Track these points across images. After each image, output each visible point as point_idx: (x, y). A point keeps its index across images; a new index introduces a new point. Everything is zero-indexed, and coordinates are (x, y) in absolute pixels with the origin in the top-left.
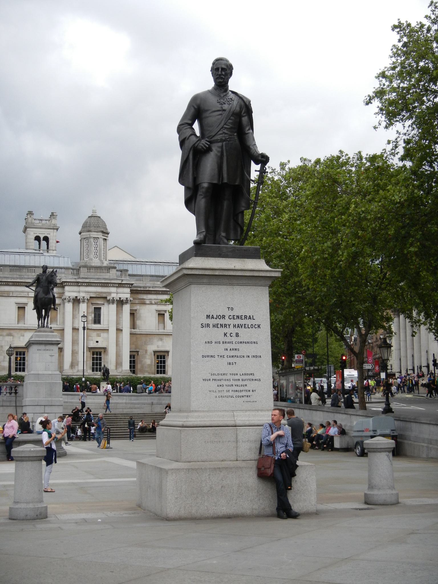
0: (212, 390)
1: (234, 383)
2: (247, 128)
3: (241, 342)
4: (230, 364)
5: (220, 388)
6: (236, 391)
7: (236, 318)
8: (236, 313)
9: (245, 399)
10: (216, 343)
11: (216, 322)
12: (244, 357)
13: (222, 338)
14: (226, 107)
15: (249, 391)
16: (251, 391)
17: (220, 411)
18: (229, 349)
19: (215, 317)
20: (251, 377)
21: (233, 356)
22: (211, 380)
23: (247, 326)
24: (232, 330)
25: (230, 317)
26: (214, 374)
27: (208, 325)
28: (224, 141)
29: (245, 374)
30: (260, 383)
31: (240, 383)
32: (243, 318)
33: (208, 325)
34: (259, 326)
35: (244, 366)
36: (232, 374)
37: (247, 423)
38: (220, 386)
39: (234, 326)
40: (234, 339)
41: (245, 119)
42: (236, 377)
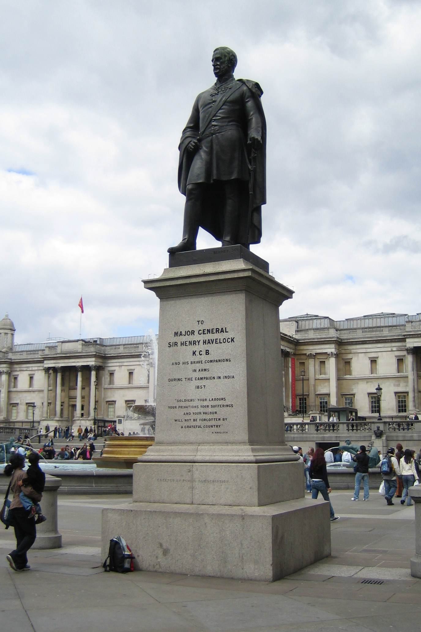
3: (211, 361)
4: (198, 387)
5: (187, 417)
6: (205, 420)
7: (206, 332)
8: (206, 326)
9: (215, 429)
12: (214, 378)
13: (190, 358)
16: (221, 419)
18: (197, 371)
19: (183, 333)
21: (201, 379)
22: (177, 407)
24: (202, 347)
26: (180, 401)
27: (176, 344)
29: (215, 399)
31: (210, 410)
33: (176, 344)
34: (232, 340)
35: (214, 389)
40: (204, 358)
42: (205, 403)
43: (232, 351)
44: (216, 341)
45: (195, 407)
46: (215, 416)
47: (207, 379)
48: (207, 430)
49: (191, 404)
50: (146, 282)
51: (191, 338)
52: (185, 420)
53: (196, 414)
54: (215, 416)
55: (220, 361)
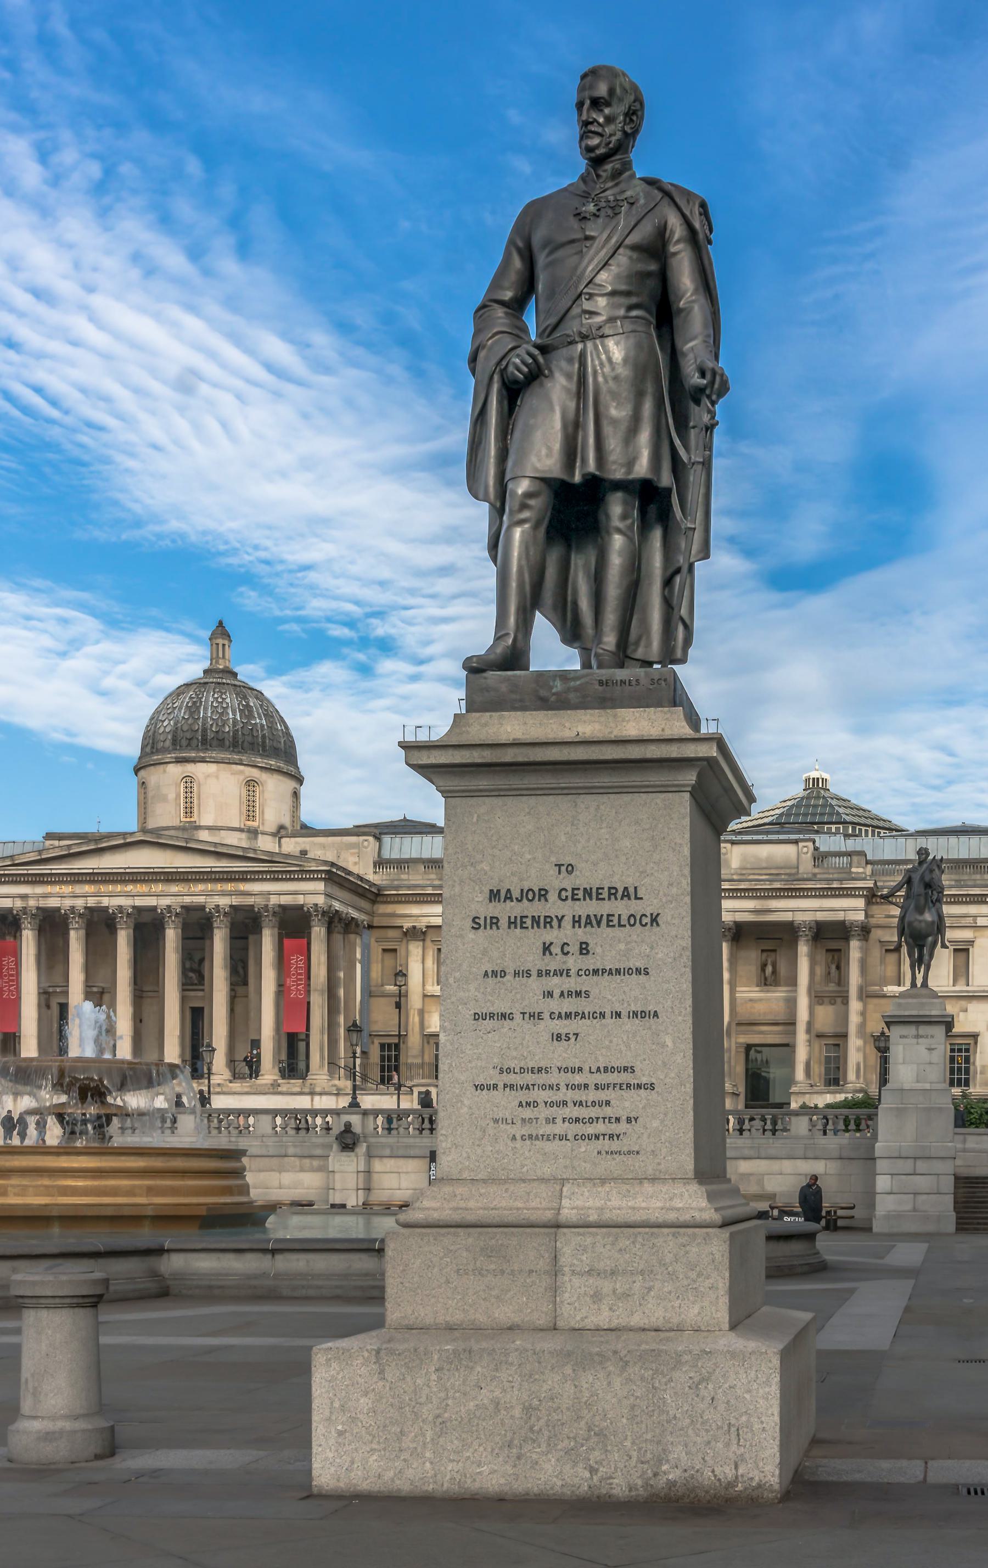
0: (501, 1115)
1: (570, 1095)
3: (596, 972)
4: (559, 1037)
5: (528, 1113)
6: (577, 1120)
7: (581, 896)
8: (584, 878)
9: (605, 1144)
10: (516, 974)
12: (603, 1015)
13: (534, 960)
17: (524, 1181)
18: (557, 993)
19: (516, 894)
20: (624, 1078)
21: (568, 1016)
24: (568, 934)
25: (564, 893)
26: (509, 1070)
27: (494, 922)
29: (606, 1070)
31: (592, 1095)
32: (605, 895)
33: (494, 922)
34: (654, 920)
36: (566, 1070)
38: (528, 1104)
39: (576, 921)
40: (573, 962)
42: (578, 1079)
43: (652, 948)
44: (609, 920)
45: (551, 1087)
46: (608, 1111)
47: (583, 1017)
48: (583, 1146)
49: (541, 1079)
50: (406, 746)
52: (523, 1120)
53: (552, 1104)
54: (608, 1111)
55: (618, 971)
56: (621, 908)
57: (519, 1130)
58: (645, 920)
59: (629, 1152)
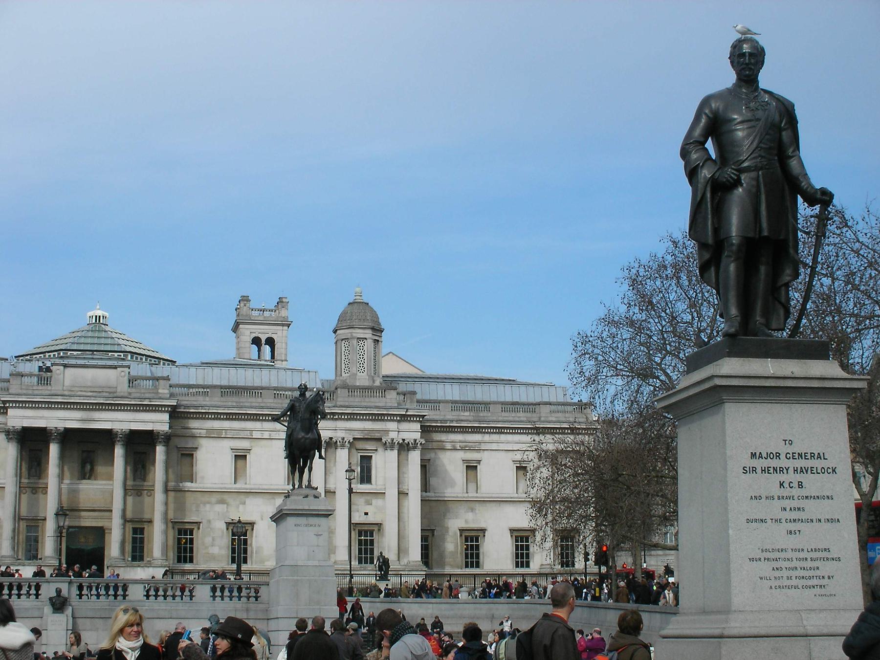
1: (798, 564)
2: (791, 150)
3: (807, 497)
5: (777, 574)
6: (803, 577)
8: (797, 448)
9: (817, 591)
10: (767, 498)
11: (764, 462)
12: (812, 521)
13: (776, 491)
14: (760, 114)
15: (823, 577)
16: (826, 577)
18: (788, 509)
19: (764, 455)
22: (763, 559)
23: (815, 469)
24: (791, 477)
27: (754, 470)
28: (761, 169)
30: (839, 564)
31: (809, 564)
32: (809, 457)
33: (754, 470)
34: (834, 471)
35: (812, 536)
37: (825, 631)
40: (796, 492)
41: (786, 135)
42: (802, 555)
46: (818, 573)
48: (807, 591)
49: (782, 555)
51: (775, 463)
54: (818, 573)
56: (817, 464)
57: (774, 583)
58: (830, 471)
59: (831, 595)
